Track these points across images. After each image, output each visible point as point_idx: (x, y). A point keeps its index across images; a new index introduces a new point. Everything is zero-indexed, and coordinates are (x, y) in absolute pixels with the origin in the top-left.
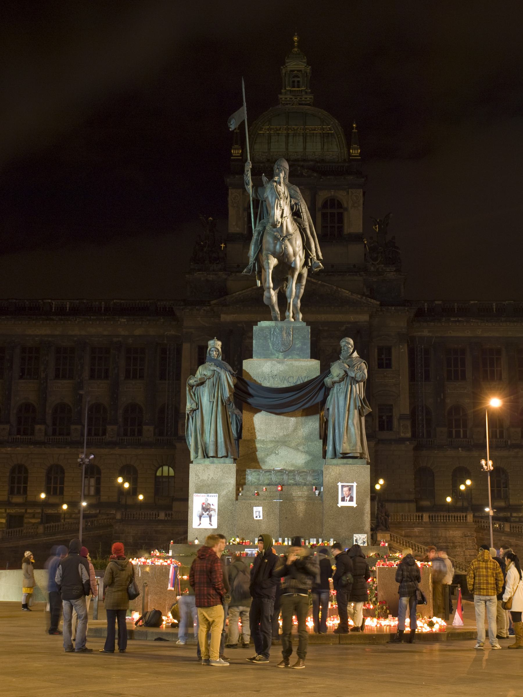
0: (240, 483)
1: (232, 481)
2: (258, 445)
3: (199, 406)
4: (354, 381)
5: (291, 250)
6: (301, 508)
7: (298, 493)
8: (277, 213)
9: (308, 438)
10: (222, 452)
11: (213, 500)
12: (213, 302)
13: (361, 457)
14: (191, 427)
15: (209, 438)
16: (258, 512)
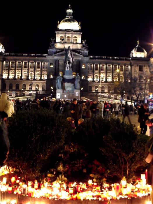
0: (63, 92)
1: (62, 92)
2: (65, 87)
3: (58, 82)
4: (78, 79)
5: (70, 60)
6: (71, 96)
7: (71, 94)
8: (69, 55)
9: (72, 86)
10: (61, 88)
11: (60, 94)
12: (53, 55)
13: (79, 89)
14: (57, 85)
15: (59, 86)
16: (65, 96)
